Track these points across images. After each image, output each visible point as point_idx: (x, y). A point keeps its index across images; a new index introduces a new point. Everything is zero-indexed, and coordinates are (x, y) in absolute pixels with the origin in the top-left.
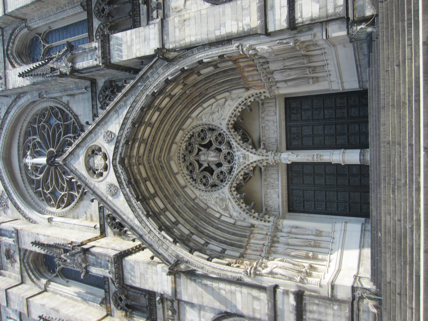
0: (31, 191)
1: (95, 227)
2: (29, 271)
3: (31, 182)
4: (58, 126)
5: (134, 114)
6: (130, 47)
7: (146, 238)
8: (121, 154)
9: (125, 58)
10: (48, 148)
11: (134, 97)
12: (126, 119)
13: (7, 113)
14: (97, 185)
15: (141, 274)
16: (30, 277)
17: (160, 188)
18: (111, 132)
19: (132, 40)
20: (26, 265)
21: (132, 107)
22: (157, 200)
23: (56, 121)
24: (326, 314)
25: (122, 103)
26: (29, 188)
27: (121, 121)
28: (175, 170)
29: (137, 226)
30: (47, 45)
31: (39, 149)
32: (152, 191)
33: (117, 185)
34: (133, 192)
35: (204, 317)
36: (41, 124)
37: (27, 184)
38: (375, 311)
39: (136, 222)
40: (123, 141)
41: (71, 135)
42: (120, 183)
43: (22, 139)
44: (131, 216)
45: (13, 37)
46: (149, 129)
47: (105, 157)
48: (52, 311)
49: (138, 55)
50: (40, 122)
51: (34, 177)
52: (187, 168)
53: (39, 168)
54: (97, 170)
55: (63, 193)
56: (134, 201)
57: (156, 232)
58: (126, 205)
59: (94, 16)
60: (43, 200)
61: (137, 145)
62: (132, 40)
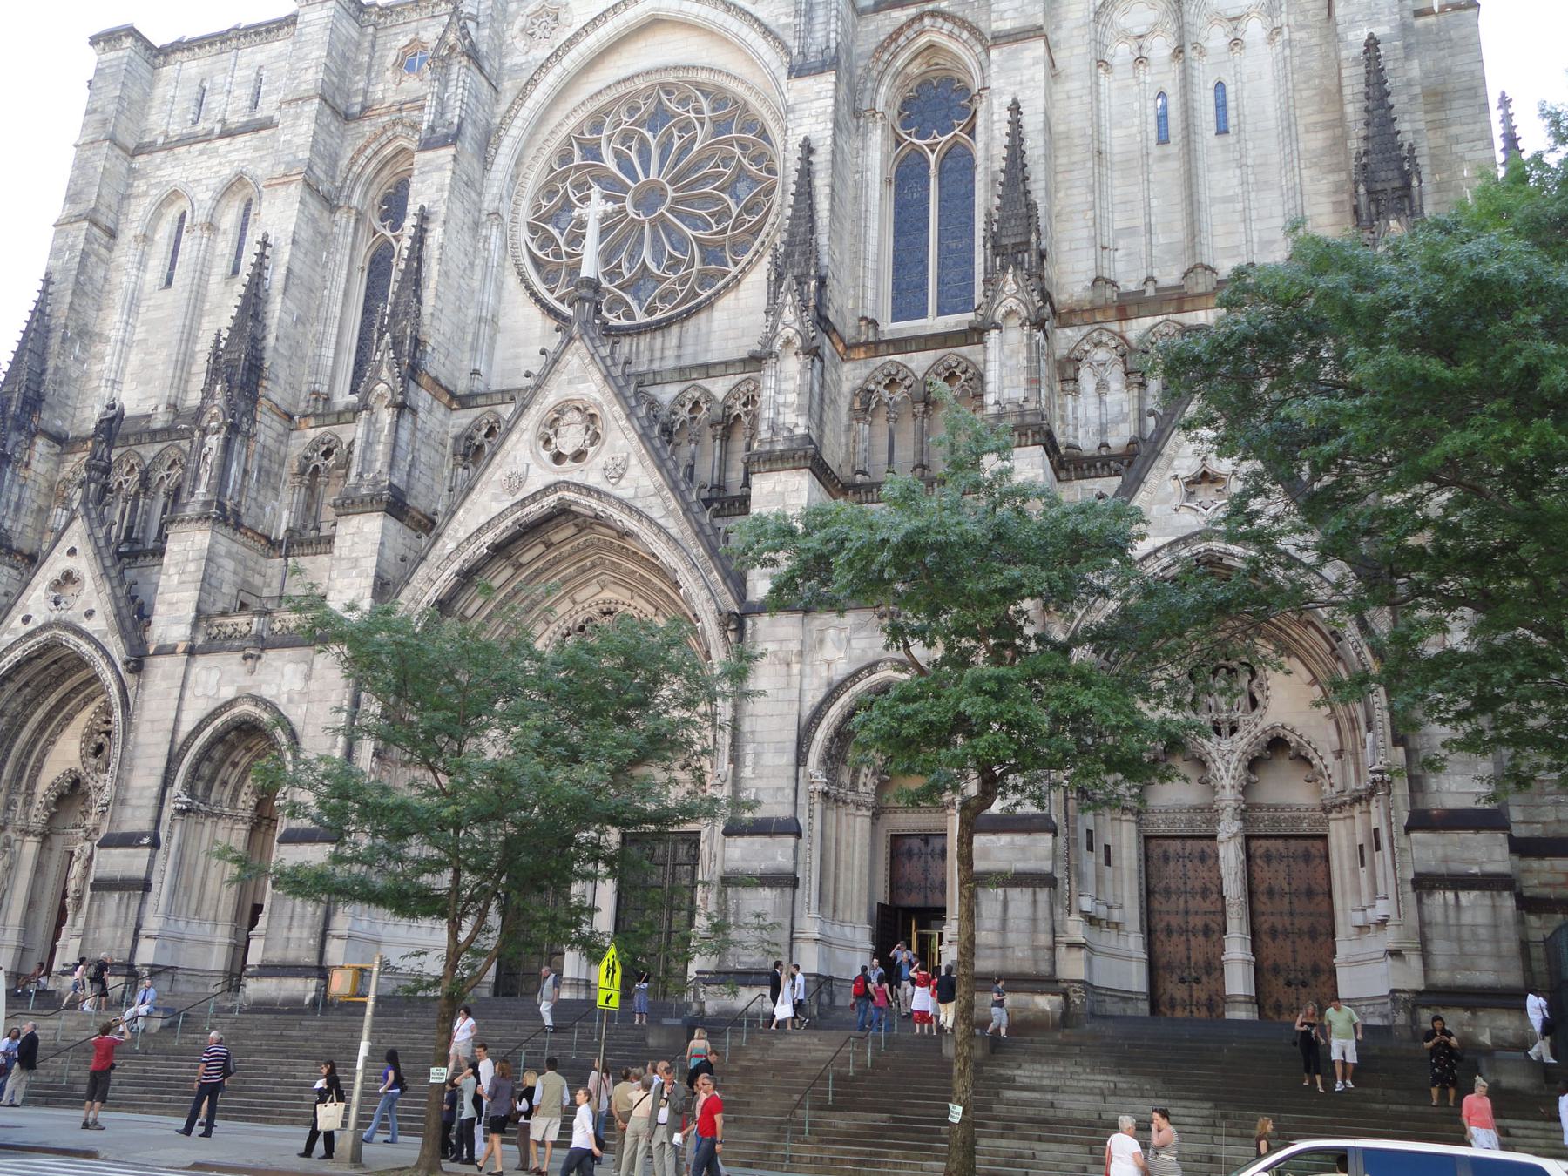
0: (573, 122)
1: (476, 372)
2: (374, 146)
4: (726, 213)
7: (422, 571)
8: (577, 503)
10: (672, 182)
11: (678, 536)
12: (640, 515)
13: (767, 31)
14: (526, 436)
15: (357, 559)
16: (360, 151)
17: (537, 574)
18: (621, 477)
20: (390, 134)
22: (508, 572)
23: (738, 201)
24: (301, 927)
25: (673, 504)
26: (581, 115)
27: (639, 505)
28: (580, 596)
29: (444, 545)
30: (932, 158)
31: (677, 143)
32: (525, 559)
33: (520, 496)
34: (504, 535)
35: (290, 700)
36: (737, 150)
37: (591, 107)
38: (307, 1001)
39: (451, 546)
41: (698, 266)
42: (522, 503)
43: (703, 77)
44: (462, 535)
45: (965, 35)
47: (579, 456)
48: (283, 270)
50: (743, 147)
51: (606, 132)
53: (630, 148)
54: (556, 433)
55: (561, 241)
56: (489, 538)
57: (432, 595)
58: (483, 520)
59: (941, 352)
60: (552, 170)
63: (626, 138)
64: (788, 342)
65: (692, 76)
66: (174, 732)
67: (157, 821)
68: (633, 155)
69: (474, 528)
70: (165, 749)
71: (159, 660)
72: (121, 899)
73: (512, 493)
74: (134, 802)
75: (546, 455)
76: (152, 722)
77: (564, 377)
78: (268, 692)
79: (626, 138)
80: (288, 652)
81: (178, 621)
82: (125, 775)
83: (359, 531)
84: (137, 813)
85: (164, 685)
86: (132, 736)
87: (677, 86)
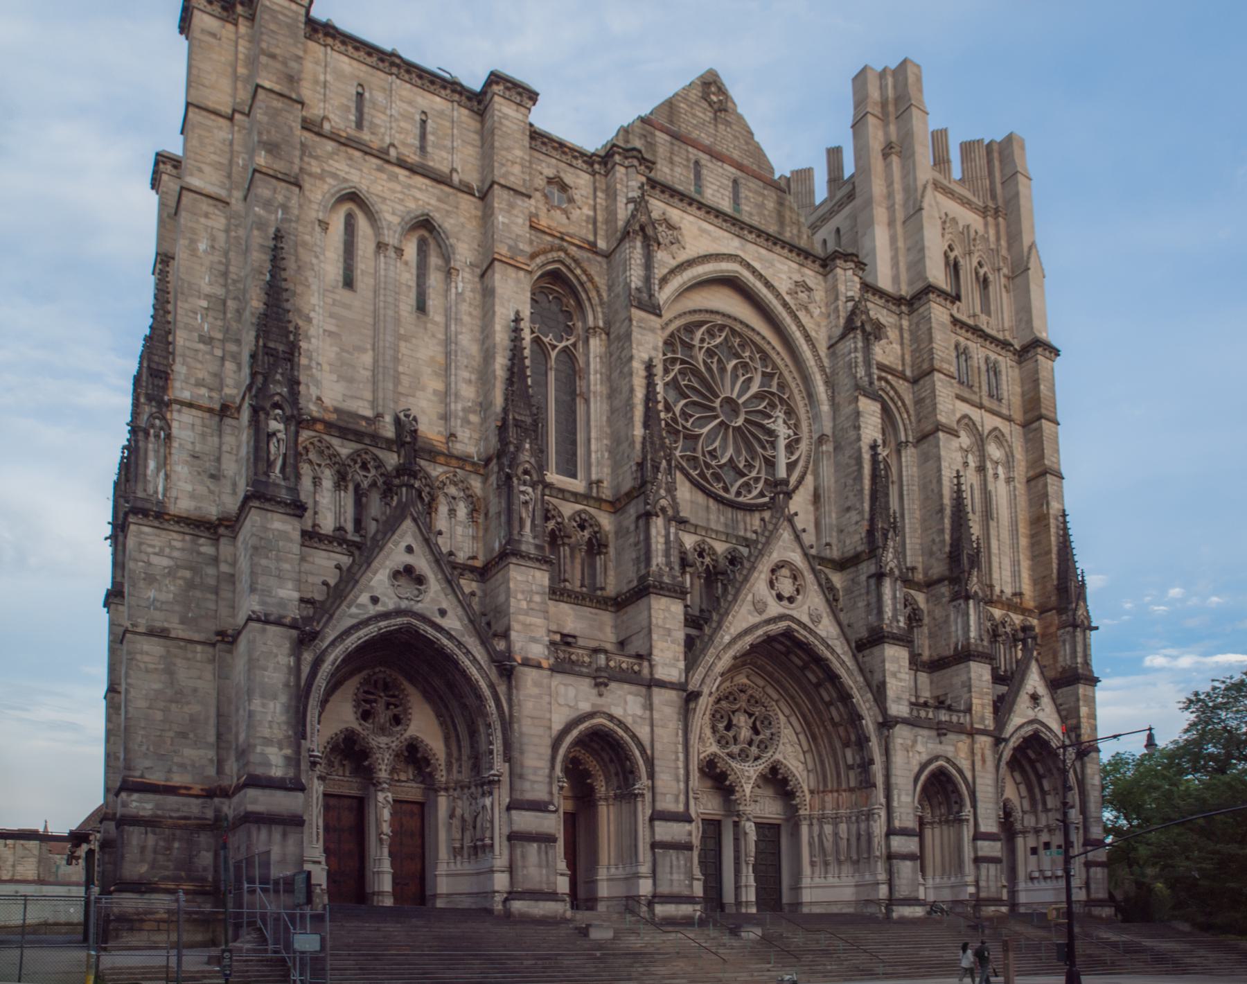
3: (690, 328)
5: (836, 665)
6: (894, 675)
9: (887, 665)
12: (833, 652)
14: (763, 576)
19: (901, 680)
21: (843, 663)
25: (846, 648)
29: (722, 637)
33: (765, 616)
35: (635, 722)
39: (727, 639)
40: (811, 639)
43: (757, 339)
46: (799, 663)
47: (791, 600)
49: (888, 686)
52: (730, 693)
56: (749, 639)
58: (745, 625)
61: (788, 643)
62: (901, 680)
63: (710, 353)
64: (891, 569)
65: (750, 334)
66: (550, 728)
67: (551, 793)
68: (714, 367)
69: (740, 630)
70: (548, 742)
71: (526, 669)
72: (539, 848)
73: (760, 613)
74: (531, 777)
75: (774, 593)
76: (532, 718)
77: (780, 543)
78: (617, 712)
79: (710, 353)
80: (626, 686)
81: (534, 640)
82: (516, 754)
83: (668, 610)
84: (535, 786)
85: (535, 691)
86: (516, 726)
87: (740, 335)
